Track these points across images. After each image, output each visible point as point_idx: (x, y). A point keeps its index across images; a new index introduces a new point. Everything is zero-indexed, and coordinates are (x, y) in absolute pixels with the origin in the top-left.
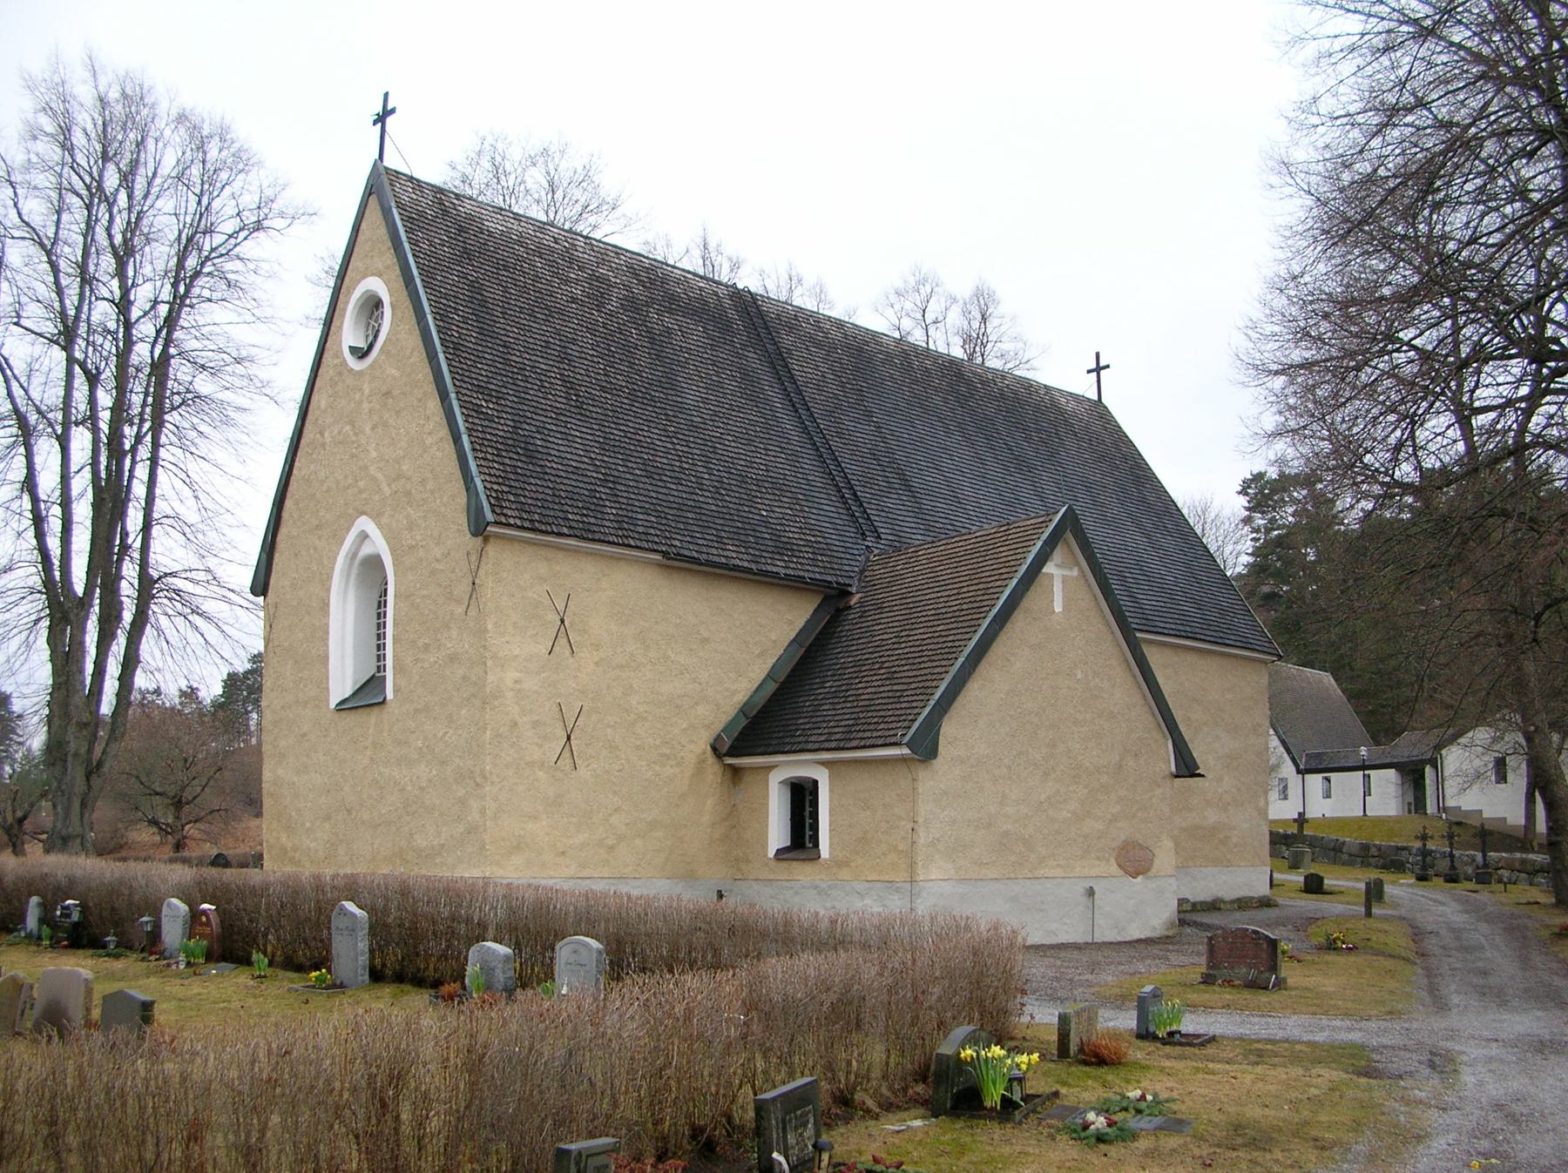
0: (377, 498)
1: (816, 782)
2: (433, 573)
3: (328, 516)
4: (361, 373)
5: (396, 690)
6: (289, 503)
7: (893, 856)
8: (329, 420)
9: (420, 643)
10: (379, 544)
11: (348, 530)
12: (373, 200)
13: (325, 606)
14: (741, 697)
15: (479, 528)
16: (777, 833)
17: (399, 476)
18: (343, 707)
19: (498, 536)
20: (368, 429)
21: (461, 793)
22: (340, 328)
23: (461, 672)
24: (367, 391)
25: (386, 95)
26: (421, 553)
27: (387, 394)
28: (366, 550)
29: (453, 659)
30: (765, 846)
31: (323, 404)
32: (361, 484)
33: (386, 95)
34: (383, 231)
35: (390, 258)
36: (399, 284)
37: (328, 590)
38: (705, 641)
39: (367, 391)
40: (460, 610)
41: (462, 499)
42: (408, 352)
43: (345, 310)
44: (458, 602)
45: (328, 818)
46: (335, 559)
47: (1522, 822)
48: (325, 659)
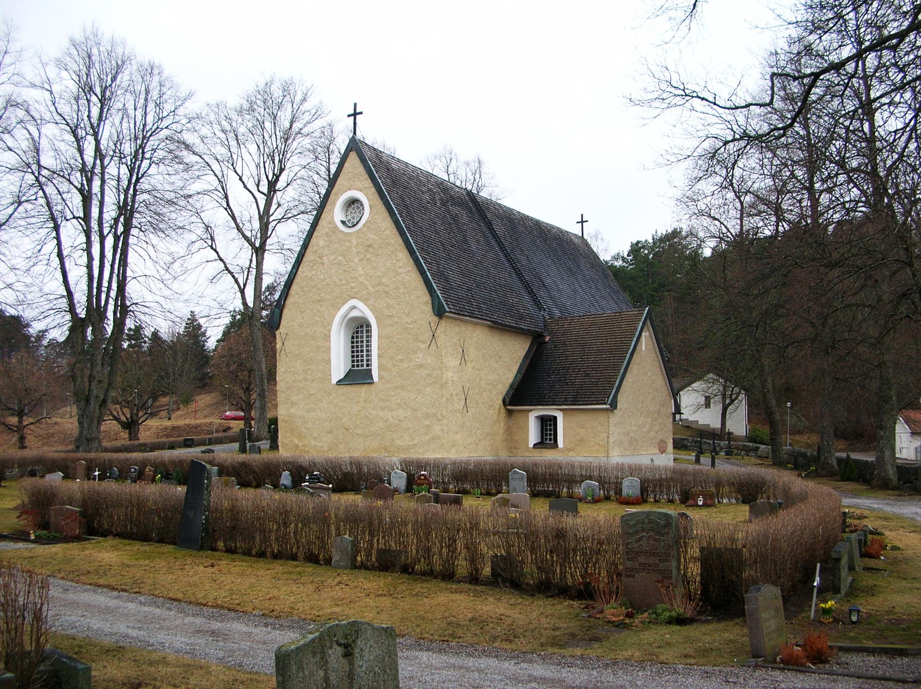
1: (555, 418)
2: (405, 328)
3: (327, 296)
4: (350, 234)
5: (380, 377)
6: (294, 287)
7: (597, 447)
8: (325, 252)
10: (364, 310)
11: (343, 304)
12: (353, 155)
13: (327, 337)
14: (511, 381)
15: (439, 312)
16: (533, 437)
17: (380, 284)
18: (340, 383)
19: (446, 317)
20: (356, 260)
21: (427, 423)
22: (332, 210)
24: (354, 243)
25: (355, 104)
28: (355, 313)
29: (420, 366)
30: (527, 442)
31: (321, 244)
32: (353, 285)
33: (355, 104)
34: (361, 169)
35: (368, 183)
36: (376, 196)
37: (329, 330)
38: (500, 357)
39: (354, 243)
40: (425, 346)
41: (427, 298)
43: (334, 203)
44: (423, 342)
45: (331, 432)
46: (334, 317)
47: (720, 426)
48: (329, 361)
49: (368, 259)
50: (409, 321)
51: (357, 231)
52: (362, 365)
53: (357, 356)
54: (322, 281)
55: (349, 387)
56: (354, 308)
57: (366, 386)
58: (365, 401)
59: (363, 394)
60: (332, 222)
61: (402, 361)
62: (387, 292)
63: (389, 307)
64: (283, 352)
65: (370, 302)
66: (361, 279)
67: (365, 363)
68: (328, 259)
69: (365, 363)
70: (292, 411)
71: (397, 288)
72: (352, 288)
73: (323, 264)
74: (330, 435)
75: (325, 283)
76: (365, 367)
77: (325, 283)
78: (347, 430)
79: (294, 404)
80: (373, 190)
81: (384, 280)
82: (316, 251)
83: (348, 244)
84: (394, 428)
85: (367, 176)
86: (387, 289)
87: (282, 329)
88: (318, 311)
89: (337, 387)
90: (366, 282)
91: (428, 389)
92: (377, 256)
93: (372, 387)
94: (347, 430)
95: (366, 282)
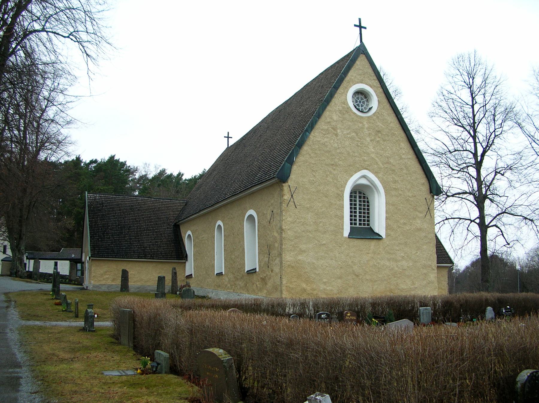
0: (376, 166)
2: (408, 200)
8: (339, 126)
9: (402, 221)
11: (356, 172)
17: (387, 163)
20: (368, 139)
21: (425, 271)
23: (424, 234)
24: (366, 126)
26: (400, 192)
27: (379, 132)
29: (420, 230)
31: (335, 117)
32: (365, 158)
39: (366, 126)
42: (389, 122)
43: (347, 89)
44: (420, 212)
45: (340, 278)
46: (347, 181)
49: (378, 142)
50: (410, 195)
51: (369, 117)
52: (355, 224)
53: (364, 217)
54: (336, 149)
55: (359, 241)
56: (364, 177)
57: (375, 241)
58: (374, 253)
59: (372, 247)
60: (345, 102)
61: (405, 224)
62: (394, 170)
63: (395, 182)
64: (291, 203)
65: (380, 175)
66: (373, 155)
67: (358, 222)
68: (342, 132)
69: (358, 222)
70: (300, 257)
71: (402, 169)
72: (364, 161)
73: (337, 135)
74: (339, 281)
75: (338, 151)
76: (358, 225)
77: (338, 151)
78: (357, 276)
79: (302, 252)
80: (381, 90)
81: (392, 161)
82: (329, 122)
83: (360, 125)
84: (399, 275)
85: (375, 78)
86: (393, 168)
87: (290, 182)
88: (331, 173)
89: (349, 240)
90: (377, 159)
91: (425, 247)
92: (384, 140)
93: (381, 242)
94: (357, 276)
95: (377, 159)
